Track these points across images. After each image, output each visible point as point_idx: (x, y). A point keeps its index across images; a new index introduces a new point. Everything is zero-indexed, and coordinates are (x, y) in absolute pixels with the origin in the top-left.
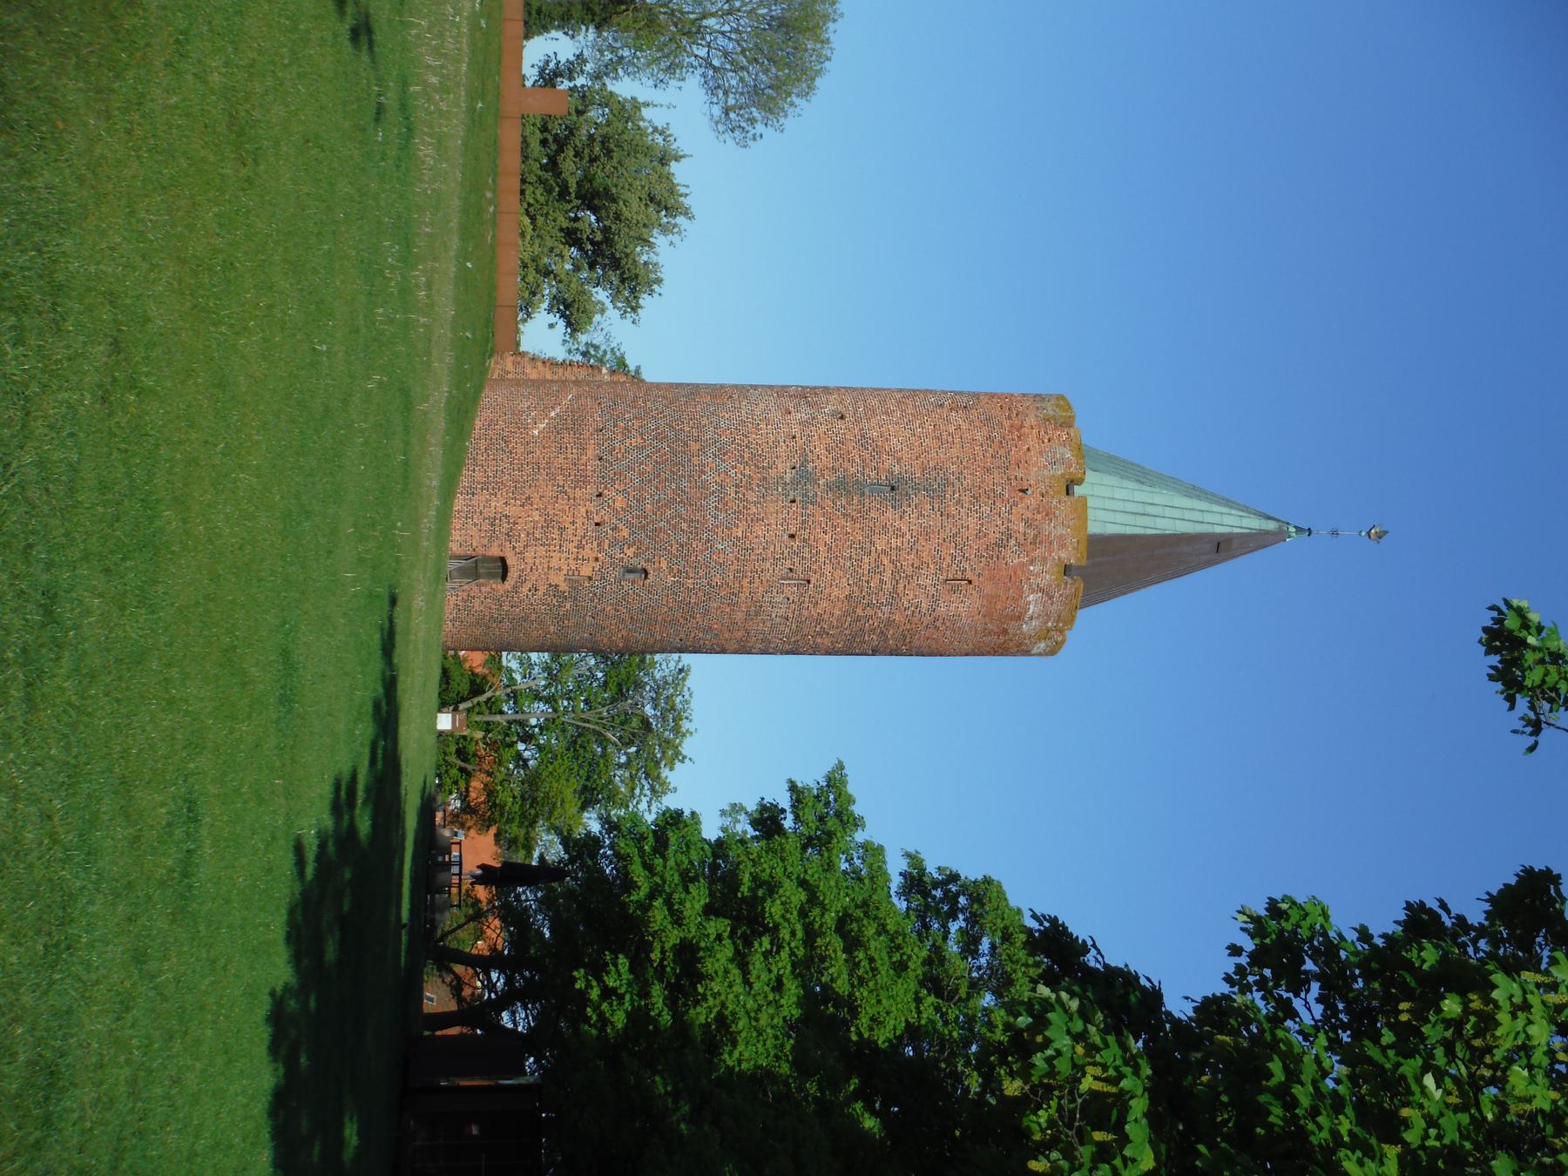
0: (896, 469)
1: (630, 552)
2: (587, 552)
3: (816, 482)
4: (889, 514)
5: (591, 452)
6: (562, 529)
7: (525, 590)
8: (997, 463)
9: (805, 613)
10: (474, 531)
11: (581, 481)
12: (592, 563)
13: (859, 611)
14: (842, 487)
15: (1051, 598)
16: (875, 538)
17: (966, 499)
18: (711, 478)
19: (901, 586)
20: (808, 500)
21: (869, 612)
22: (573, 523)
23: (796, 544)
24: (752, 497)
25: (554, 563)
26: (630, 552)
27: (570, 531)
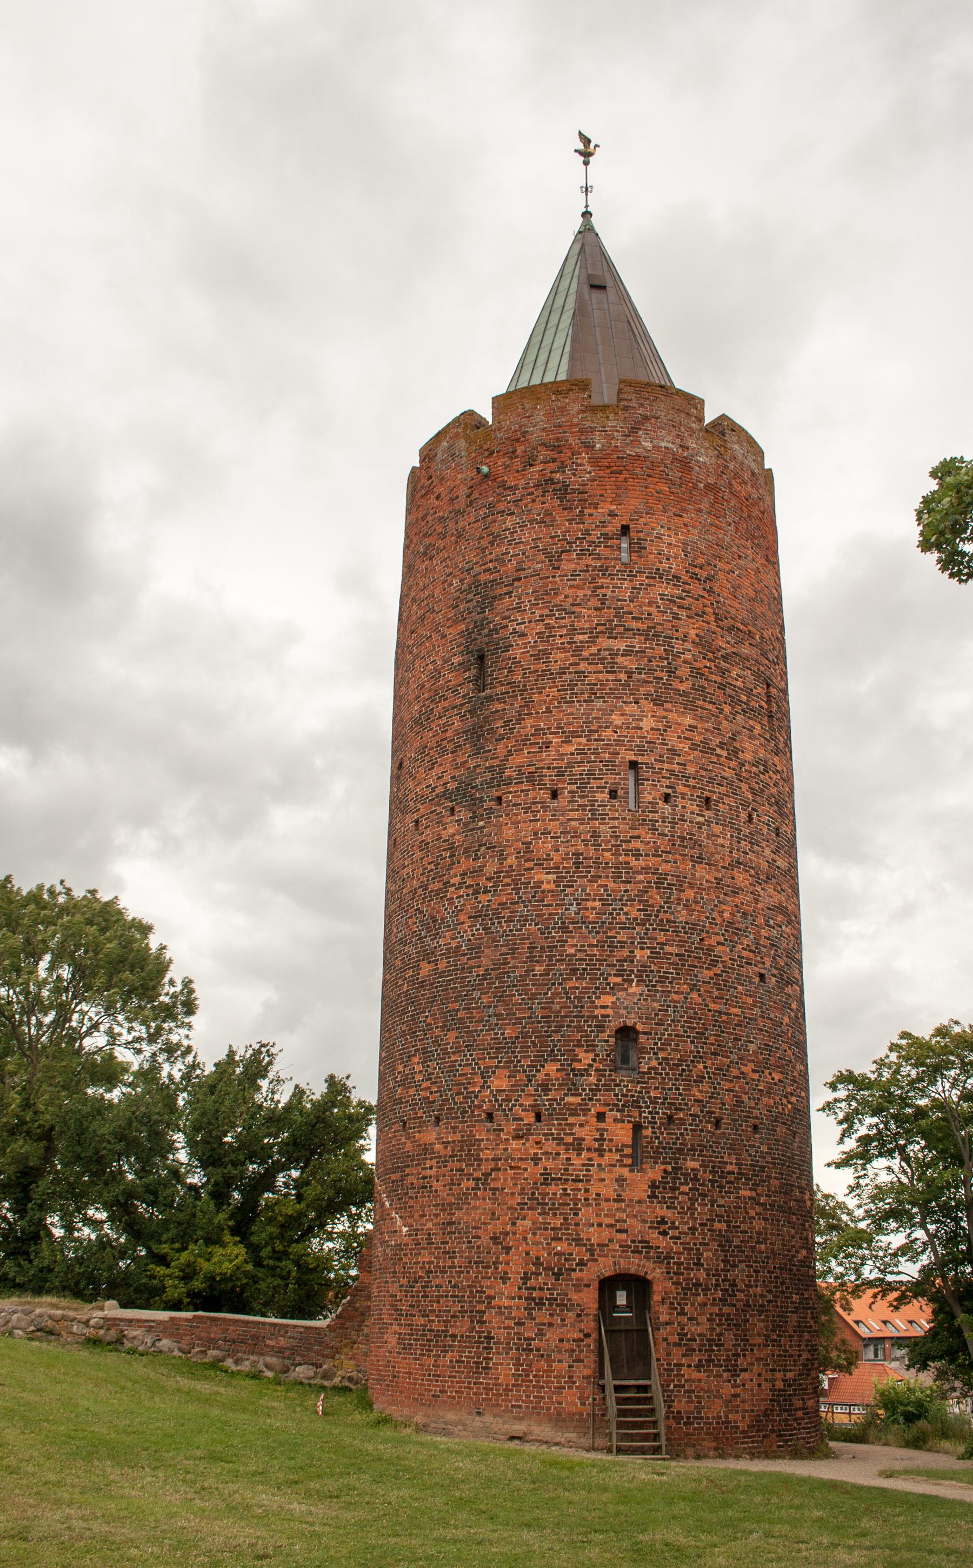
0: (456, 660)
1: (586, 1058)
2: (587, 1134)
3: (473, 771)
4: (516, 652)
5: (430, 1135)
6: (547, 1178)
7: (663, 1243)
8: (451, 525)
9: (691, 770)
10: (552, 1336)
11: (467, 1149)
12: (608, 1124)
13: (682, 687)
14: (477, 736)
15: (646, 418)
16: (555, 668)
17: (497, 551)
18: (469, 931)
19: (634, 625)
20: (498, 778)
21: (684, 671)
22: (536, 1160)
23: (567, 789)
24: (491, 868)
25: (609, 1190)
26: (586, 1058)
27: (550, 1164)
